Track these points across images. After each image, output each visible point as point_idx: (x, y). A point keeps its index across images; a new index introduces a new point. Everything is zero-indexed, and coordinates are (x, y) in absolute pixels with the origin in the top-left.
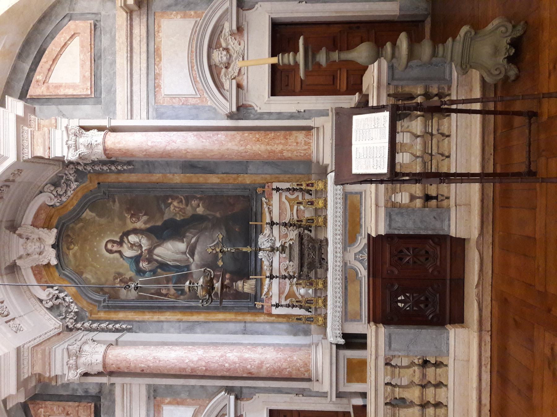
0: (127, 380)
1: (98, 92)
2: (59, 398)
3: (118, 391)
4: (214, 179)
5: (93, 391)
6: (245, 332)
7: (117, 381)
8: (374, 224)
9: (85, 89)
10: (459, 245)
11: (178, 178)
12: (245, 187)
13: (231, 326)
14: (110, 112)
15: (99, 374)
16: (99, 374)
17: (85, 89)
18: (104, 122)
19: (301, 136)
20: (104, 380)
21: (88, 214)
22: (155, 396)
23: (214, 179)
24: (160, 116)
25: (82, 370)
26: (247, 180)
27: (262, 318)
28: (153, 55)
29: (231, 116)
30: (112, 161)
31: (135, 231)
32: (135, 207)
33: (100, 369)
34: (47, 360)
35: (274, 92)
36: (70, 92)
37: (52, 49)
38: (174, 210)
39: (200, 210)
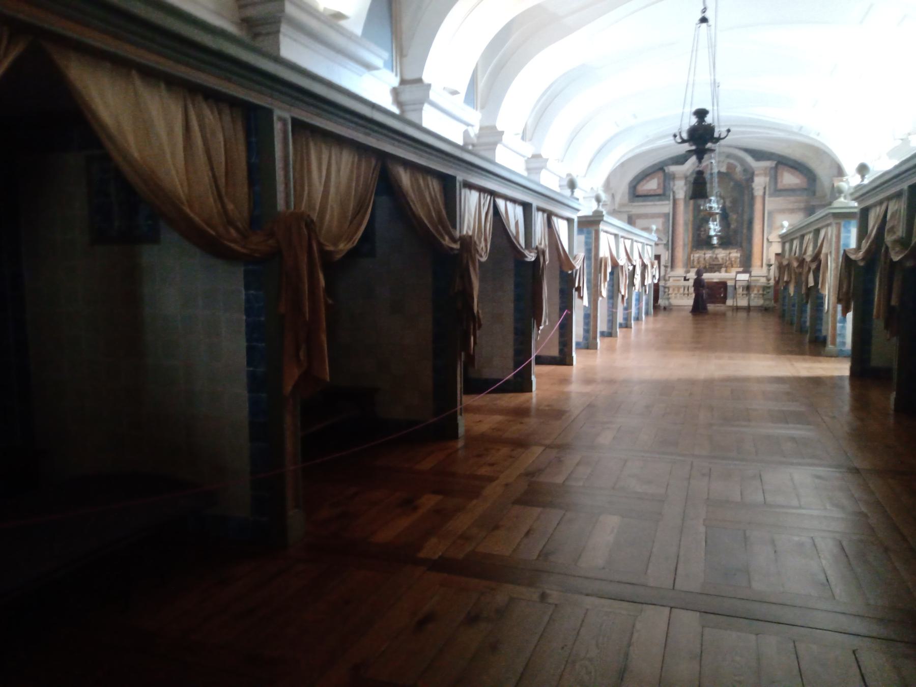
0: (671, 206)
1: (778, 191)
2: (664, 181)
3: (667, 202)
4: (745, 231)
5: (667, 193)
6: (684, 245)
7: (671, 201)
8: (730, 283)
9: (780, 186)
10: (724, 302)
11: (746, 217)
12: (741, 243)
13: (686, 240)
14: (771, 195)
15: (674, 197)
16: (674, 197)
17: (780, 186)
18: (767, 193)
19: (759, 263)
20: (671, 197)
21: (732, 184)
22: (666, 215)
23: (745, 231)
24: (770, 213)
25: (677, 192)
26: (744, 245)
27: (689, 250)
28: (792, 211)
29: (768, 240)
30: (752, 198)
31: (724, 203)
32: (735, 202)
33: (677, 197)
34: (680, 178)
35: (777, 255)
36: (779, 180)
37: (797, 173)
38: (733, 217)
39: (732, 226)
